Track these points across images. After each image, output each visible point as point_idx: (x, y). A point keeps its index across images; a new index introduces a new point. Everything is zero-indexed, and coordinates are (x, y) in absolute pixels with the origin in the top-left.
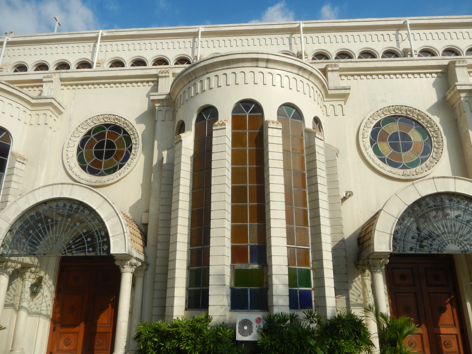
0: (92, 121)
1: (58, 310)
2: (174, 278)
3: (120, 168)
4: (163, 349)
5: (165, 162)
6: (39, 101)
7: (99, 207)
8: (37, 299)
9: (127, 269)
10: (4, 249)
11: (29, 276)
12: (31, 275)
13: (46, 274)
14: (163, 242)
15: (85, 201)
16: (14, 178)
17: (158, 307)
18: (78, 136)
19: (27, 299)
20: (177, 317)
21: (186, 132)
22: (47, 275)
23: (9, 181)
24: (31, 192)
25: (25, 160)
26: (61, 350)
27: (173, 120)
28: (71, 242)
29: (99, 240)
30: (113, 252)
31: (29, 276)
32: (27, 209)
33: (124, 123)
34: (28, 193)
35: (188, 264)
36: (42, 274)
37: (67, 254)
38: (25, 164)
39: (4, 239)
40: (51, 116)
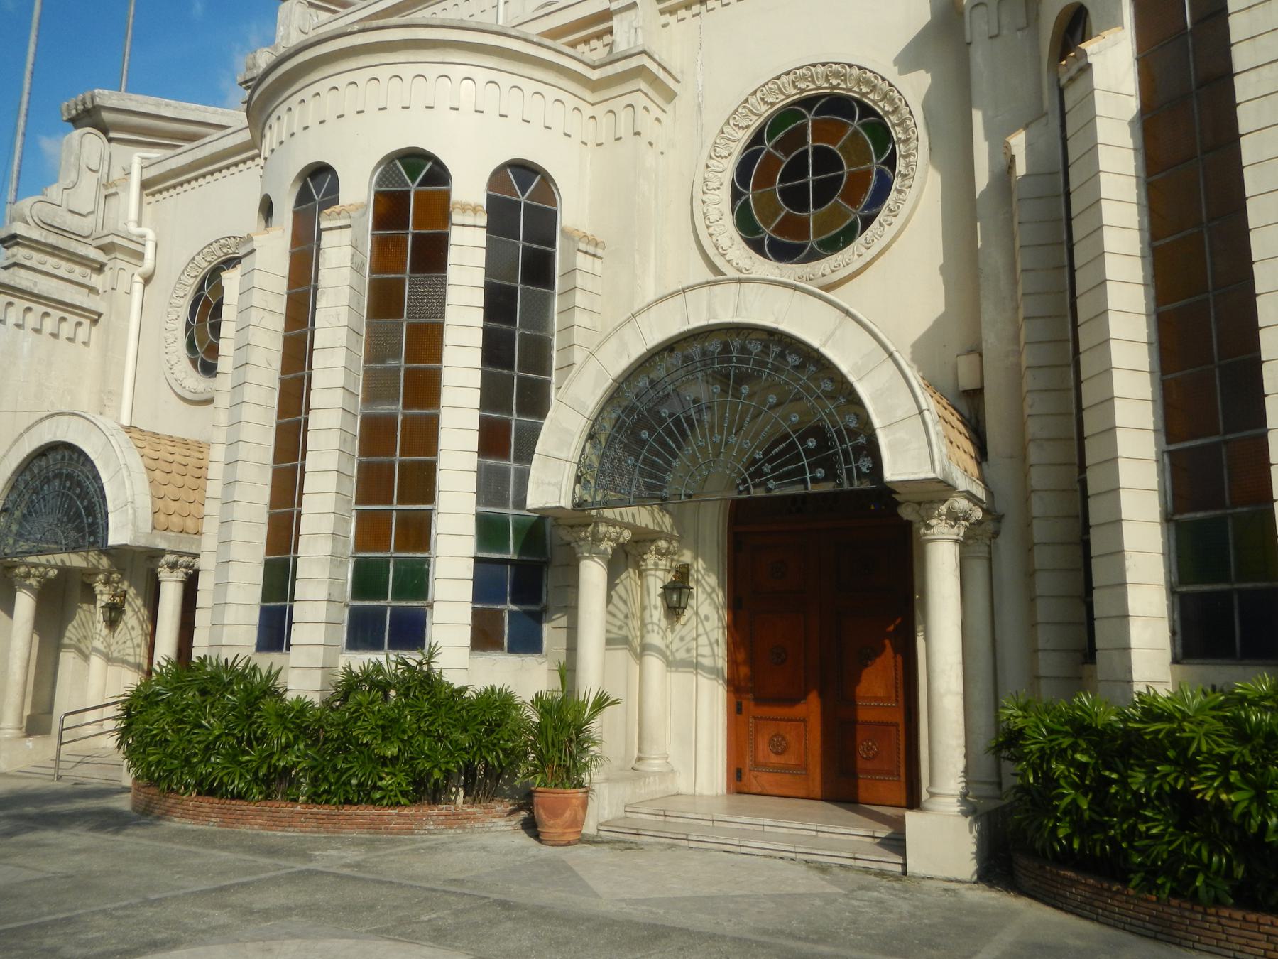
0: (762, 99)
1: (741, 656)
2: (1121, 552)
3: (864, 228)
4: (1117, 793)
5: (1021, 169)
6: (610, 70)
7: (829, 338)
8: (685, 625)
9: (941, 529)
10: (584, 487)
11: (656, 565)
12: (661, 560)
13: (696, 558)
14: (1048, 440)
15: (784, 327)
16: (579, 299)
17: (1053, 650)
18: (729, 155)
19: (660, 627)
20: (1147, 687)
21: (1104, 34)
22: (700, 561)
23: (569, 310)
24: (628, 320)
25: (599, 246)
26: (765, 765)
27: (1028, 25)
28: (759, 455)
29: (842, 441)
30: (892, 475)
31: (656, 565)
32: (624, 371)
33: (859, 82)
34: (622, 325)
35: (1164, 503)
36: (687, 557)
37: (752, 490)
38: (601, 258)
39: (580, 461)
40: (645, 108)
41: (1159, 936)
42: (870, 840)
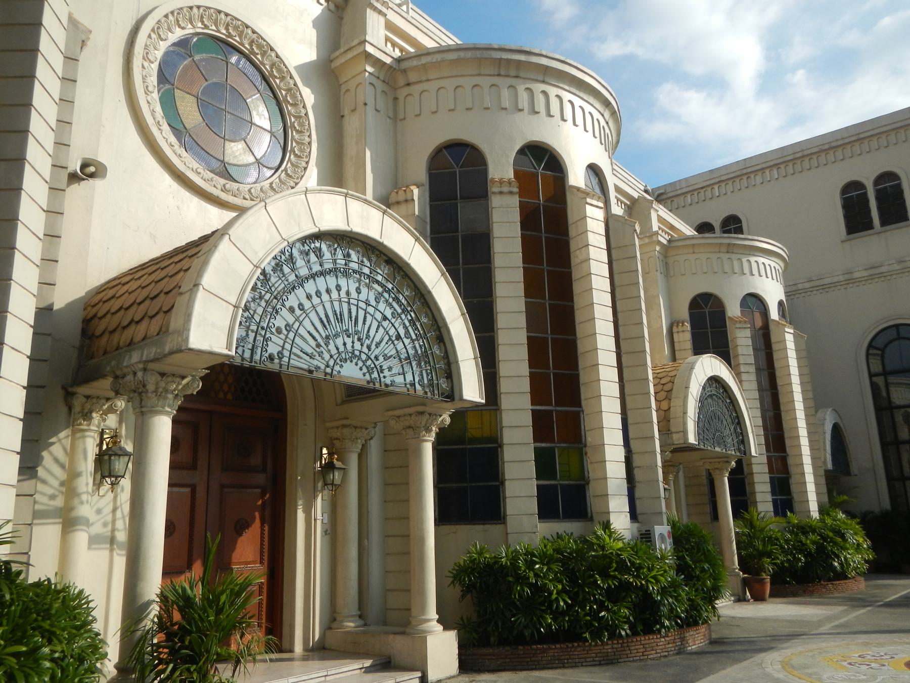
33: (273, 65)
41: (602, 662)
42: (359, 671)
